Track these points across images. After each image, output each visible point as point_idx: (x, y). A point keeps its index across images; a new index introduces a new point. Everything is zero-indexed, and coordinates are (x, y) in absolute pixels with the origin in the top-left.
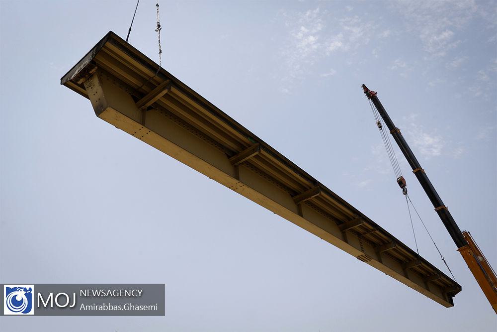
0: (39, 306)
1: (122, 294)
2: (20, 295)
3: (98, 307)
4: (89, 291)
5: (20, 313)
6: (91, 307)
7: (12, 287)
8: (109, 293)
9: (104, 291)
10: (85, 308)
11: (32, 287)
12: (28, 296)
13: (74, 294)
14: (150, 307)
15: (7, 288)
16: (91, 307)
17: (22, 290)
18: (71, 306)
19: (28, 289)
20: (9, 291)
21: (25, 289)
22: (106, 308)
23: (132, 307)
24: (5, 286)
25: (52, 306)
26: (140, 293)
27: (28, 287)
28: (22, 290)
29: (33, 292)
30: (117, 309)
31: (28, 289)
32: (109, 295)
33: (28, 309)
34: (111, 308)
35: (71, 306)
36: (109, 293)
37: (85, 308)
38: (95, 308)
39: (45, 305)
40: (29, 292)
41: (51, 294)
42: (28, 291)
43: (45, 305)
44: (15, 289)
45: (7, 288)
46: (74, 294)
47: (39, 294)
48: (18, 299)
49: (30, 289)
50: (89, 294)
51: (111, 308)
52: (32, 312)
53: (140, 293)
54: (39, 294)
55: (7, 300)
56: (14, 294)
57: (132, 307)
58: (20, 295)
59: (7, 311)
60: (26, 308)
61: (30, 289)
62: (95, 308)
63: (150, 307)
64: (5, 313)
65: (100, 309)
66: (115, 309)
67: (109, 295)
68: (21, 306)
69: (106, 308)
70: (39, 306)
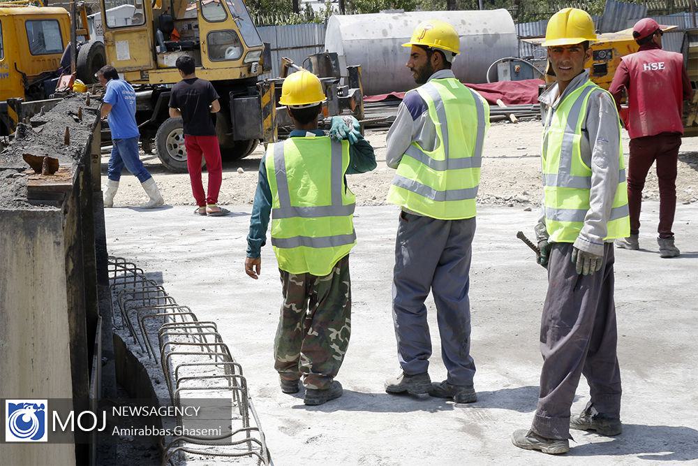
0: (54, 430)
1: (171, 413)
2: (29, 415)
3: (137, 432)
4: (126, 409)
5: (29, 440)
6: (127, 432)
7: (16, 402)
8: (153, 411)
9: (145, 409)
10: (120, 431)
11: (45, 402)
12: (40, 415)
13: (104, 412)
14: (211, 432)
15: (9, 404)
16: (127, 432)
17: (32, 407)
18: (99, 430)
19: (39, 406)
20: (13, 408)
21: (35, 406)
22: (148, 432)
23: (186, 432)
24: (8, 402)
25: (73, 430)
26: (196, 411)
27: (39, 402)
28: (32, 407)
29: (46, 410)
30: (164, 434)
31: (39, 406)
32: (154, 414)
33: (40, 434)
34: (156, 432)
35: (99, 430)
36: (153, 411)
37: (120, 431)
38: (134, 432)
39: (63, 429)
40: (41, 409)
41: (72, 413)
42: (39, 408)
43: (63, 429)
44: (21, 406)
45: (9, 404)
46: (104, 412)
47: (55, 413)
48: (26, 419)
49: (42, 406)
50: (126, 413)
51: (156, 432)
52: (45, 438)
53: (196, 411)
54: (55, 413)
55: (10, 421)
56: (19, 412)
57: (186, 432)
58: (29, 415)
59: (9, 437)
60: (36, 432)
61: (42, 406)
62: (134, 432)
63: (211, 432)
64: (7, 440)
65: (141, 433)
66: (162, 433)
67: (154, 414)
68: (30, 430)
69: (148, 432)
70: (54, 430)
